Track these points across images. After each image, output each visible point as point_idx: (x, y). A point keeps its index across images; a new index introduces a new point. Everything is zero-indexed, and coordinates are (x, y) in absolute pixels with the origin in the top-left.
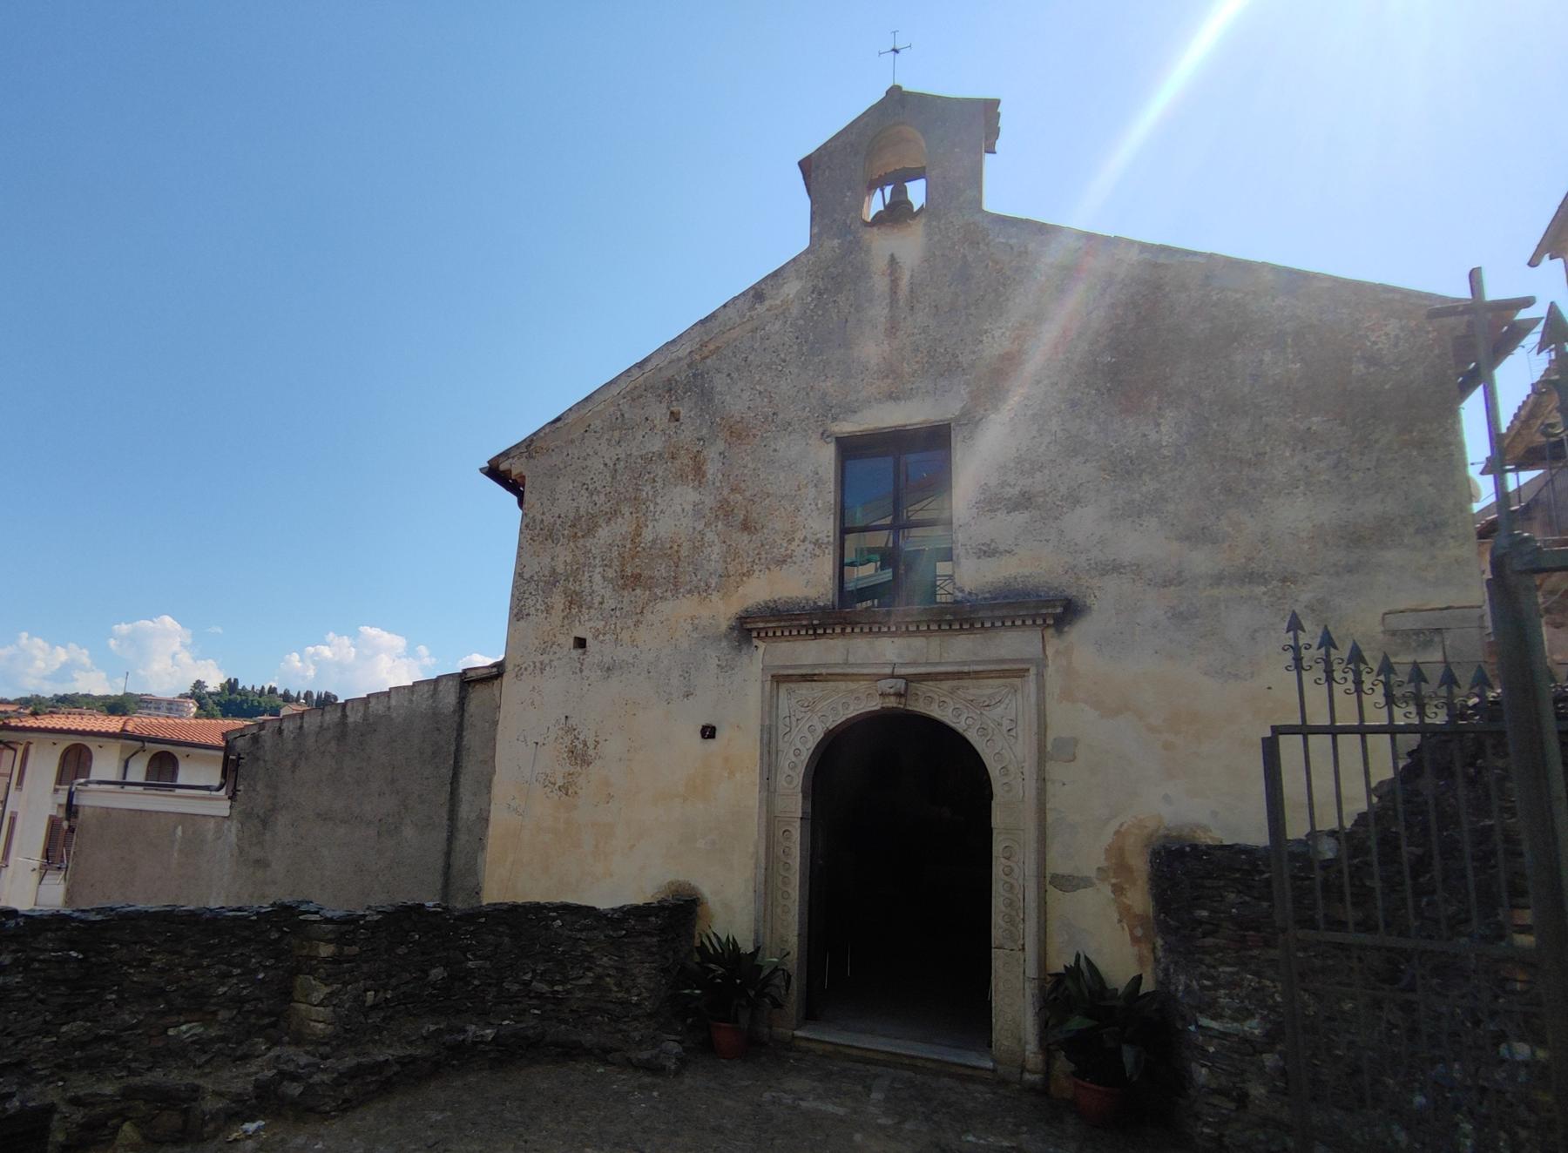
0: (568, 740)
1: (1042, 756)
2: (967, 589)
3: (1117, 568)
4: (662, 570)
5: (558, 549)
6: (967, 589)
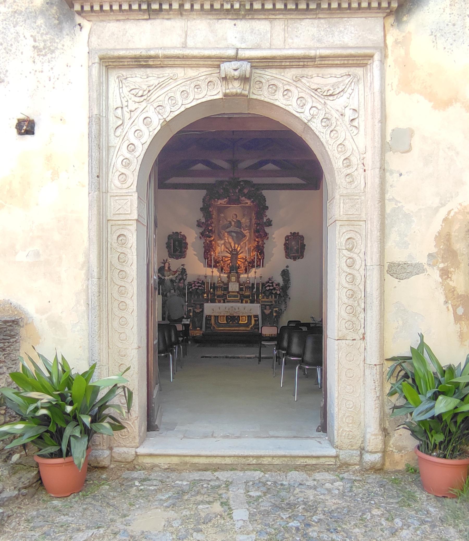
1: (384, 148)
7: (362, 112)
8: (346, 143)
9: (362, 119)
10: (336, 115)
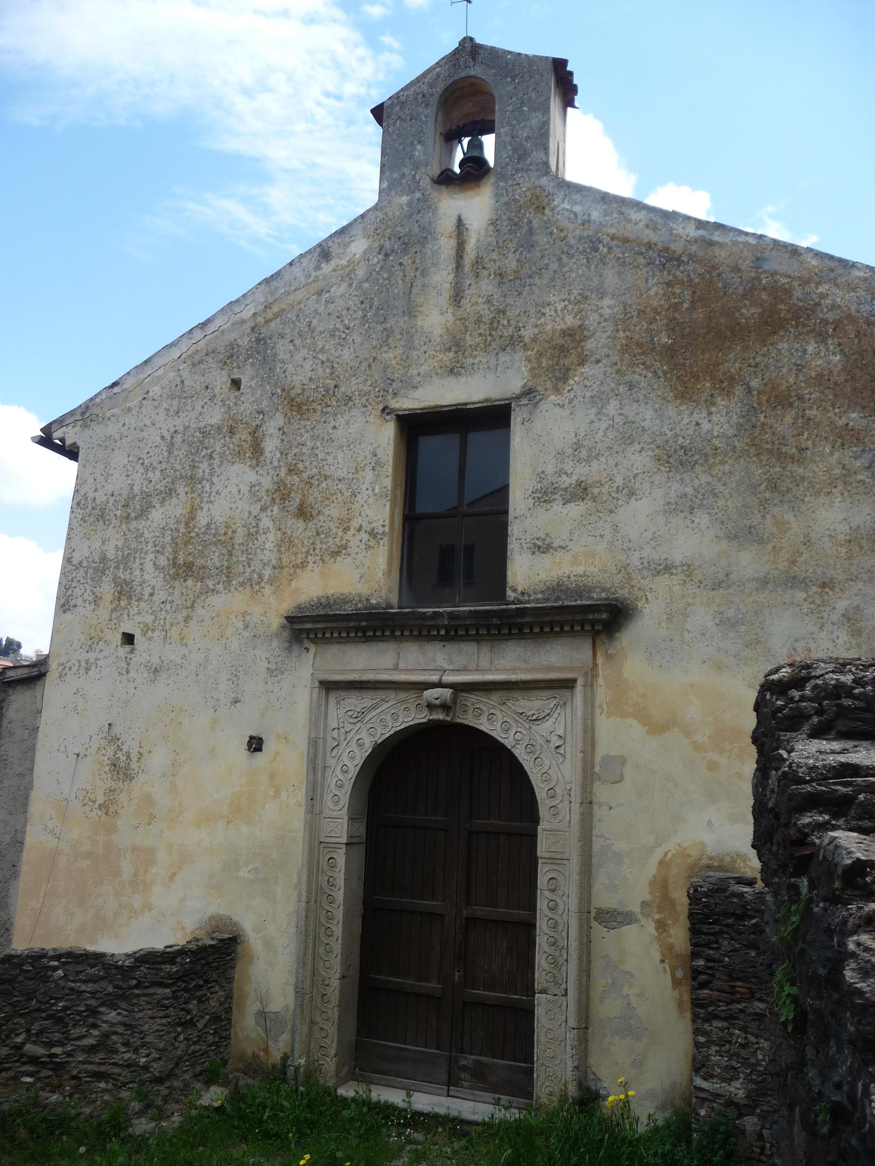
0: (110, 751)
2: (520, 589)
3: (668, 569)
4: (215, 558)
5: (111, 531)
6: (520, 589)
7: (568, 738)
8: (551, 772)
9: (568, 745)
10: (540, 741)
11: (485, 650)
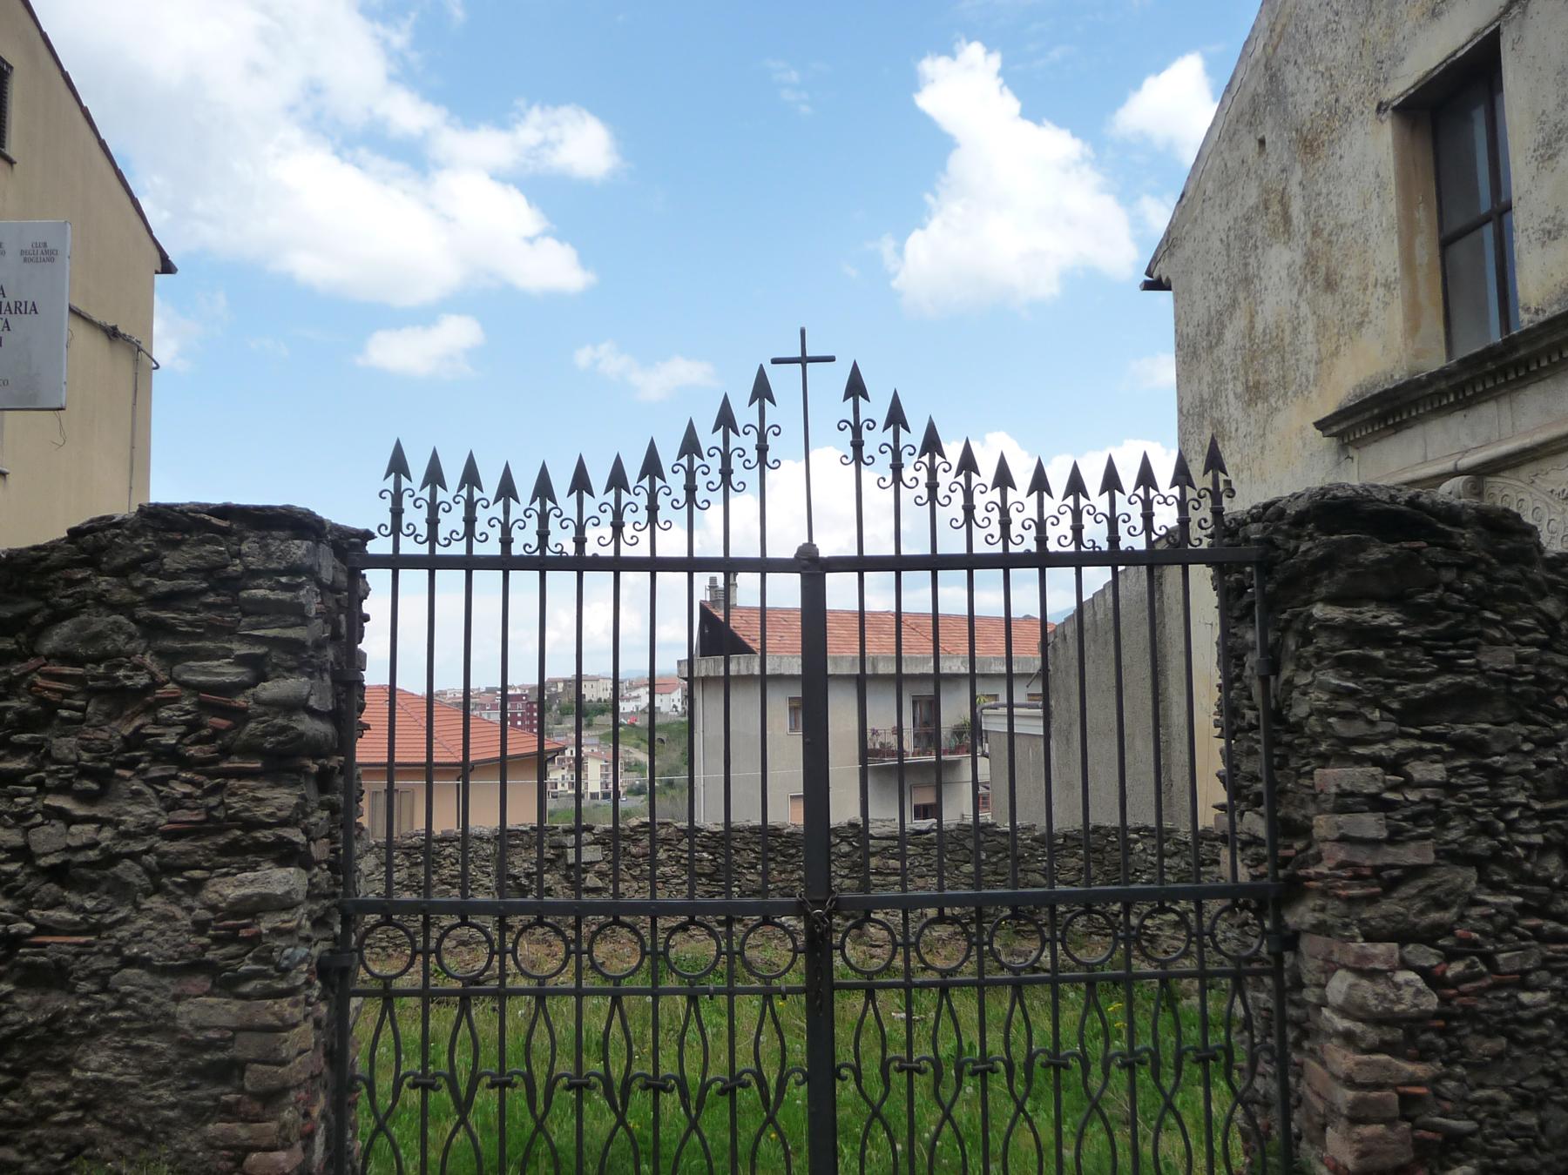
2: (1533, 306)
6: (1533, 306)
11: (1505, 405)
